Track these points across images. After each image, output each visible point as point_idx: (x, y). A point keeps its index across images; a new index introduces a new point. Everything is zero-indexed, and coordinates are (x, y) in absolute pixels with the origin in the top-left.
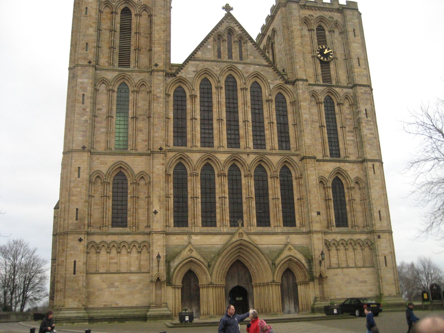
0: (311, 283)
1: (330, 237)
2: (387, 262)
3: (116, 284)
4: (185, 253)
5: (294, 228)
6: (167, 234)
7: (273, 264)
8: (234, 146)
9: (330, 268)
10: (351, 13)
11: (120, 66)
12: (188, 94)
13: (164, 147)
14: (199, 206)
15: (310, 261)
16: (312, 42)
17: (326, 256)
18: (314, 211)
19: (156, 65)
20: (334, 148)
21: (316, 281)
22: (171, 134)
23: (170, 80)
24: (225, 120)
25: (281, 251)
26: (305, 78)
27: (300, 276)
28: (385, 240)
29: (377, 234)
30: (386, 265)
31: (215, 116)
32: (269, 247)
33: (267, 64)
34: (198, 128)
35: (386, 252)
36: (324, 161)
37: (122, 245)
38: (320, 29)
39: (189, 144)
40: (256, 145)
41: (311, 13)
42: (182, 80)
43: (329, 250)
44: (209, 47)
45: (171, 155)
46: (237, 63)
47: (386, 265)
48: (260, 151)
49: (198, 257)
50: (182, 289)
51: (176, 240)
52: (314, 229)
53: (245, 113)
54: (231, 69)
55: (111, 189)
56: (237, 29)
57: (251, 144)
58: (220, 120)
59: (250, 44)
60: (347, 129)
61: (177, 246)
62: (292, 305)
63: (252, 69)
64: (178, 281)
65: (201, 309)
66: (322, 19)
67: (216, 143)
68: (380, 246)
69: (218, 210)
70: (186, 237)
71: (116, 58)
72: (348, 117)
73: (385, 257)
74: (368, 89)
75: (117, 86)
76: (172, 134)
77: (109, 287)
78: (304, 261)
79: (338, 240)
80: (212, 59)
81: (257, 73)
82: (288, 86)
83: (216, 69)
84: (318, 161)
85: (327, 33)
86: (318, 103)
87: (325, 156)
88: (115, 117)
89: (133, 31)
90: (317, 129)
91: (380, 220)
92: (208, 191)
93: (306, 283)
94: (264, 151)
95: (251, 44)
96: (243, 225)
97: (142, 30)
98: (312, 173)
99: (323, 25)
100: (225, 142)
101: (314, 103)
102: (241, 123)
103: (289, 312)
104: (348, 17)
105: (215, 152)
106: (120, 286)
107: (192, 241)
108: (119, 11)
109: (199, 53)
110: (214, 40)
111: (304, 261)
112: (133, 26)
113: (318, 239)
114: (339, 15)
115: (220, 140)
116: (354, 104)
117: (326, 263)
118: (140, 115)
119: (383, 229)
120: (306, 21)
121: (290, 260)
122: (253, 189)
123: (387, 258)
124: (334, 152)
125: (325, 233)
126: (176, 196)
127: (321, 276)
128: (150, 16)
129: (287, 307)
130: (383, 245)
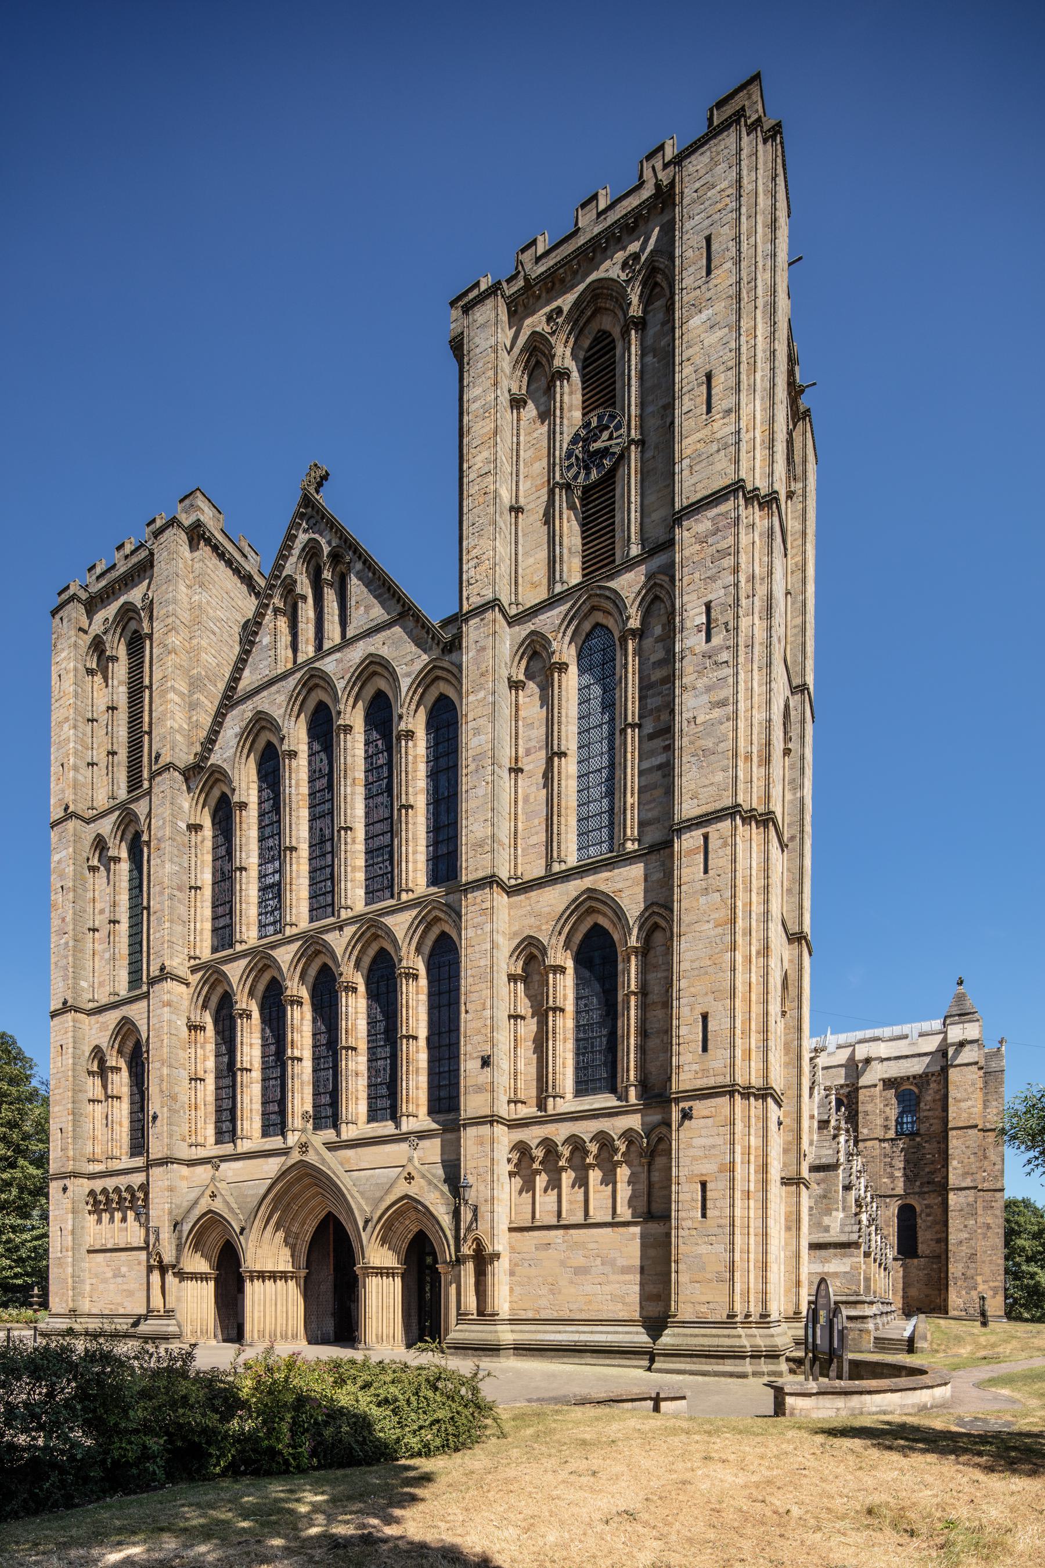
2: (709, 1204)
3: (124, 1269)
18: (475, 1055)
28: (710, 1121)
29: (682, 1105)
30: (704, 1215)
35: (707, 1168)
47: (704, 1215)
68: (690, 1146)
73: (704, 1185)
77: (115, 1276)
81: (371, 659)
91: (705, 1049)
98: (479, 932)
106: (127, 1274)
119: (711, 1082)
123: (709, 1186)
130: (697, 1142)
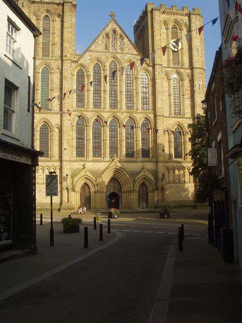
0: (156, 192)
1: (169, 165)
4: (83, 173)
5: (148, 159)
6: (72, 161)
7: (134, 180)
8: (114, 107)
9: (169, 183)
10: (195, 17)
11: (43, 56)
12: (85, 74)
13: (71, 109)
14: (91, 145)
15: (156, 177)
16: (168, 38)
17: (166, 176)
19: (66, 56)
20: (177, 109)
21: (159, 190)
22: (75, 100)
23: (74, 65)
24: (108, 91)
25: (139, 172)
26: (160, 64)
27: (150, 189)
31: (102, 89)
32: (132, 170)
33: (137, 53)
34: (91, 97)
36: (169, 117)
37: (46, 167)
38: (174, 27)
39: (86, 107)
40: (128, 107)
41: (168, 17)
42: (82, 66)
43: (169, 172)
44: (100, 42)
45: (74, 113)
46: (117, 53)
48: (129, 111)
49: (90, 175)
50: (81, 194)
51: (77, 165)
52: (160, 160)
53: (121, 87)
54: (114, 57)
55: (39, 135)
56: (118, 29)
57: (124, 107)
58: (105, 91)
59: (126, 40)
60: (186, 97)
61: (77, 169)
62: (145, 204)
63: (127, 57)
64: (78, 188)
65: (92, 205)
66: (176, 22)
67: (102, 106)
69: (102, 148)
70: (83, 163)
71: (40, 50)
72: (187, 88)
74: (201, 70)
75: (41, 69)
76: (75, 100)
78: (152, 179)
79: (174, 166)
80: (102, 51)
82: (149, 68)
83: (103, 57)
84: (165, 117)
85: (179, 31)
86: (169, 79)
87: (170, 114)
88: (40, 90)
89: (51, 32)
90: (167, 97)
92: (97, 135)
93: (153, 191)
94: (132, 110)
95: (127, 40)
96: (117, 156)
97: (56, 32)
99: (176, 25)
100: (108, 106)
101: (166, 79)
102: (119, 93)
103: (143, 208)
104: (192, 21)
105: (102, 112)
107: (86, 166)
108: (42, 18)
109: (93, 47)
110: (103, 37)
111: (152, 179)
112: (51, 29)
113: (162, 166)
114: (187, 18)
115: (105, 104)
116: (192, 81)
117: (167, 180)
118: (56, 88)
120: (166, 23)
121: (144, 178)
122: (124, 135)
124: (177, 111)
125: (167, 162)
126: (78, 138)
127: (162, 188)
128: (62, 22)
129: (141, 205)
